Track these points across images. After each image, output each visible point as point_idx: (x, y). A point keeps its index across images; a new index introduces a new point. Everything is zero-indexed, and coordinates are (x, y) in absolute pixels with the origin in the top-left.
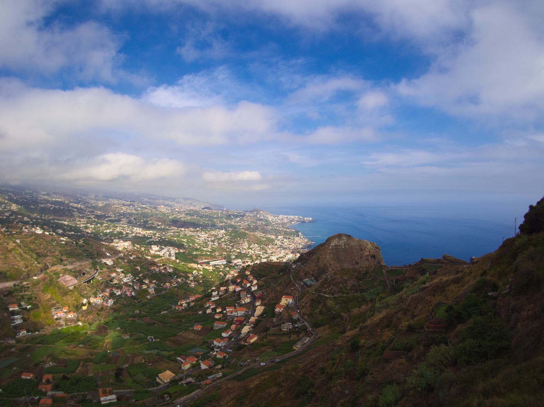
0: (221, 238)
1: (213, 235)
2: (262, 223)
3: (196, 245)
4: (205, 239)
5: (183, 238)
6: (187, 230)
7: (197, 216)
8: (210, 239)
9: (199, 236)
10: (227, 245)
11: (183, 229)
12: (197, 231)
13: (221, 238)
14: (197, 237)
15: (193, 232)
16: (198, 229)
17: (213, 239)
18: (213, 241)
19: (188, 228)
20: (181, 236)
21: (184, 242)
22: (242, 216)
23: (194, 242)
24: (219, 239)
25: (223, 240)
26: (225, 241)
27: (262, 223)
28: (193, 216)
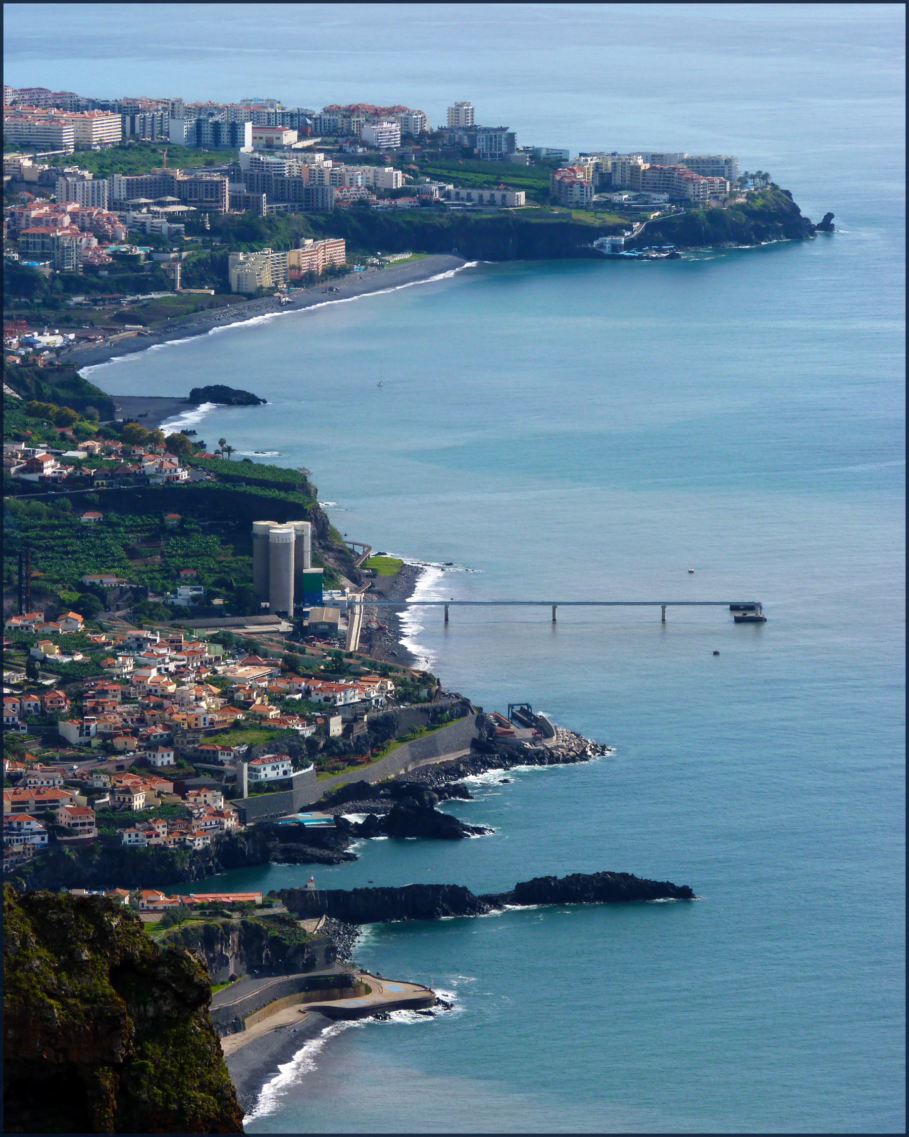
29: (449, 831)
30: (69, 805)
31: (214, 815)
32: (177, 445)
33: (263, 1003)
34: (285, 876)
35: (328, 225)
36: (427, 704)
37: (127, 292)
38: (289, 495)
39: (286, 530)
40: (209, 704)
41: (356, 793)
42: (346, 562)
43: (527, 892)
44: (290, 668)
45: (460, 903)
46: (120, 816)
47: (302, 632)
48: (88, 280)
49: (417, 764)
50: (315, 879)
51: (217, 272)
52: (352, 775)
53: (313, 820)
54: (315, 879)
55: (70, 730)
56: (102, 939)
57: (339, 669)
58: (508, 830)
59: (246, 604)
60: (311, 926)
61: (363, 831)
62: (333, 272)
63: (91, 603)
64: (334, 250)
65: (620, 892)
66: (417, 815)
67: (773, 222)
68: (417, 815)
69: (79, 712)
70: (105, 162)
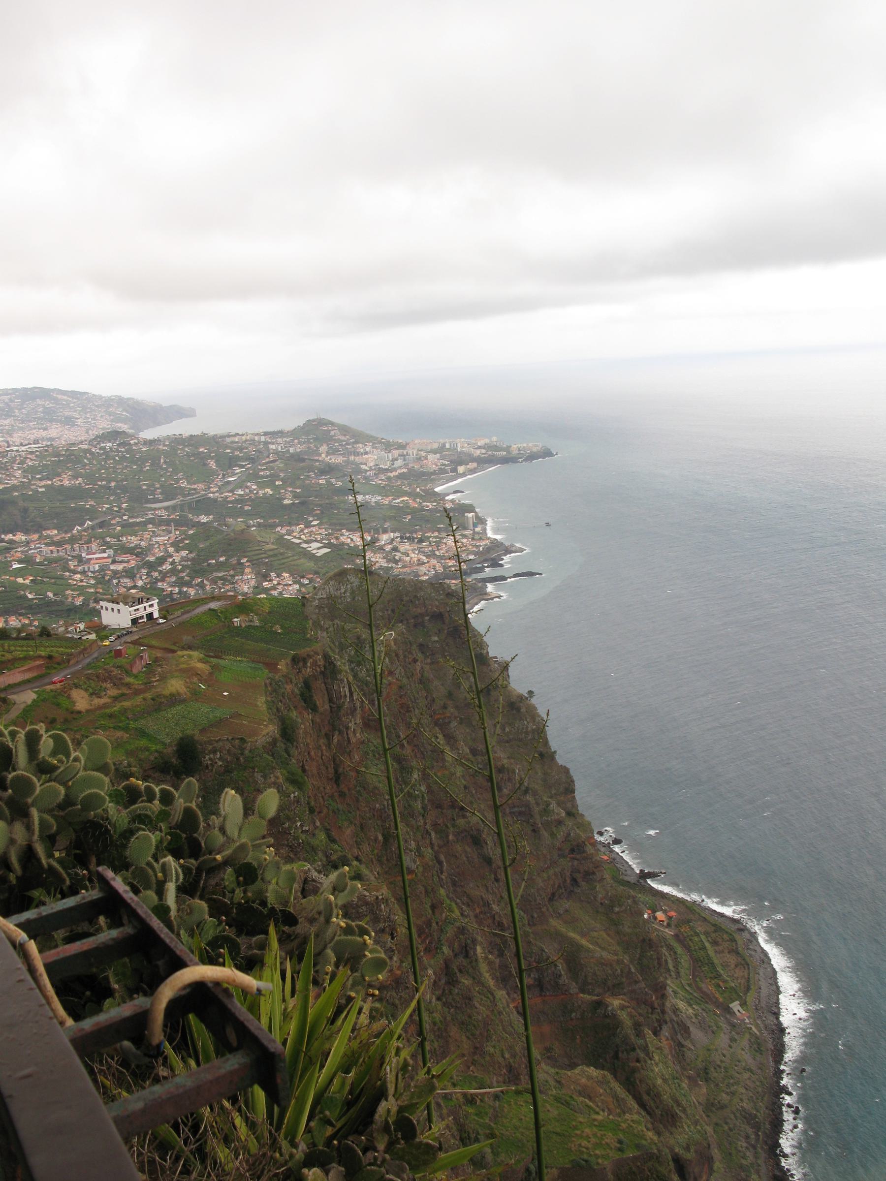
0: (161, 561)
1: (131, 551)
2: (329, 483)
3: (68, 592)
4: (103, 569)
5: (19, 573)
6: (35, 536)
7: (75, 477)
8: (120, 567)
10: (181, 583)
11: (20, 537)
12: (73, 540)
13: (161, 561)
14: (72, 564)
15: (59, 544)
17: (133, 563)
18: (130, 574)
19: (39, 528)
21: (24, 587)
22: (252, 460)
23: (61, 584)
24: (151, 566)
25: (167, 567)
26: (174, 571)
27: (329, 483)
28: (59, 475)
30: (438, 566)
32: (452, 501)
33: (473, 598)
34: (475, 576)
35: (473, 460)
37: (441, 474)
38: (470, 508)
39: (470, 515)
41: (485, 561)
44: (473, 539)
45: (504, 578)
47: (474, 533)
48: (434, 473)
49: (493, 554)
50: (479, 576)
51: (455, 470)
52: (485, 557)
53: (478, 566)
54: (479, 576)
55: (437, 553)
56: (444, 590)
59: (465, 528)
60: (480, 585)
61: (487, 567)
62: (475, 468)
63: (439, 530)
64: (475, 465)
65: (530, 574)
66: (495, 564)
67: (547, 453)
68: (495, 564)
69: (438, 550)
70: (434, 452)
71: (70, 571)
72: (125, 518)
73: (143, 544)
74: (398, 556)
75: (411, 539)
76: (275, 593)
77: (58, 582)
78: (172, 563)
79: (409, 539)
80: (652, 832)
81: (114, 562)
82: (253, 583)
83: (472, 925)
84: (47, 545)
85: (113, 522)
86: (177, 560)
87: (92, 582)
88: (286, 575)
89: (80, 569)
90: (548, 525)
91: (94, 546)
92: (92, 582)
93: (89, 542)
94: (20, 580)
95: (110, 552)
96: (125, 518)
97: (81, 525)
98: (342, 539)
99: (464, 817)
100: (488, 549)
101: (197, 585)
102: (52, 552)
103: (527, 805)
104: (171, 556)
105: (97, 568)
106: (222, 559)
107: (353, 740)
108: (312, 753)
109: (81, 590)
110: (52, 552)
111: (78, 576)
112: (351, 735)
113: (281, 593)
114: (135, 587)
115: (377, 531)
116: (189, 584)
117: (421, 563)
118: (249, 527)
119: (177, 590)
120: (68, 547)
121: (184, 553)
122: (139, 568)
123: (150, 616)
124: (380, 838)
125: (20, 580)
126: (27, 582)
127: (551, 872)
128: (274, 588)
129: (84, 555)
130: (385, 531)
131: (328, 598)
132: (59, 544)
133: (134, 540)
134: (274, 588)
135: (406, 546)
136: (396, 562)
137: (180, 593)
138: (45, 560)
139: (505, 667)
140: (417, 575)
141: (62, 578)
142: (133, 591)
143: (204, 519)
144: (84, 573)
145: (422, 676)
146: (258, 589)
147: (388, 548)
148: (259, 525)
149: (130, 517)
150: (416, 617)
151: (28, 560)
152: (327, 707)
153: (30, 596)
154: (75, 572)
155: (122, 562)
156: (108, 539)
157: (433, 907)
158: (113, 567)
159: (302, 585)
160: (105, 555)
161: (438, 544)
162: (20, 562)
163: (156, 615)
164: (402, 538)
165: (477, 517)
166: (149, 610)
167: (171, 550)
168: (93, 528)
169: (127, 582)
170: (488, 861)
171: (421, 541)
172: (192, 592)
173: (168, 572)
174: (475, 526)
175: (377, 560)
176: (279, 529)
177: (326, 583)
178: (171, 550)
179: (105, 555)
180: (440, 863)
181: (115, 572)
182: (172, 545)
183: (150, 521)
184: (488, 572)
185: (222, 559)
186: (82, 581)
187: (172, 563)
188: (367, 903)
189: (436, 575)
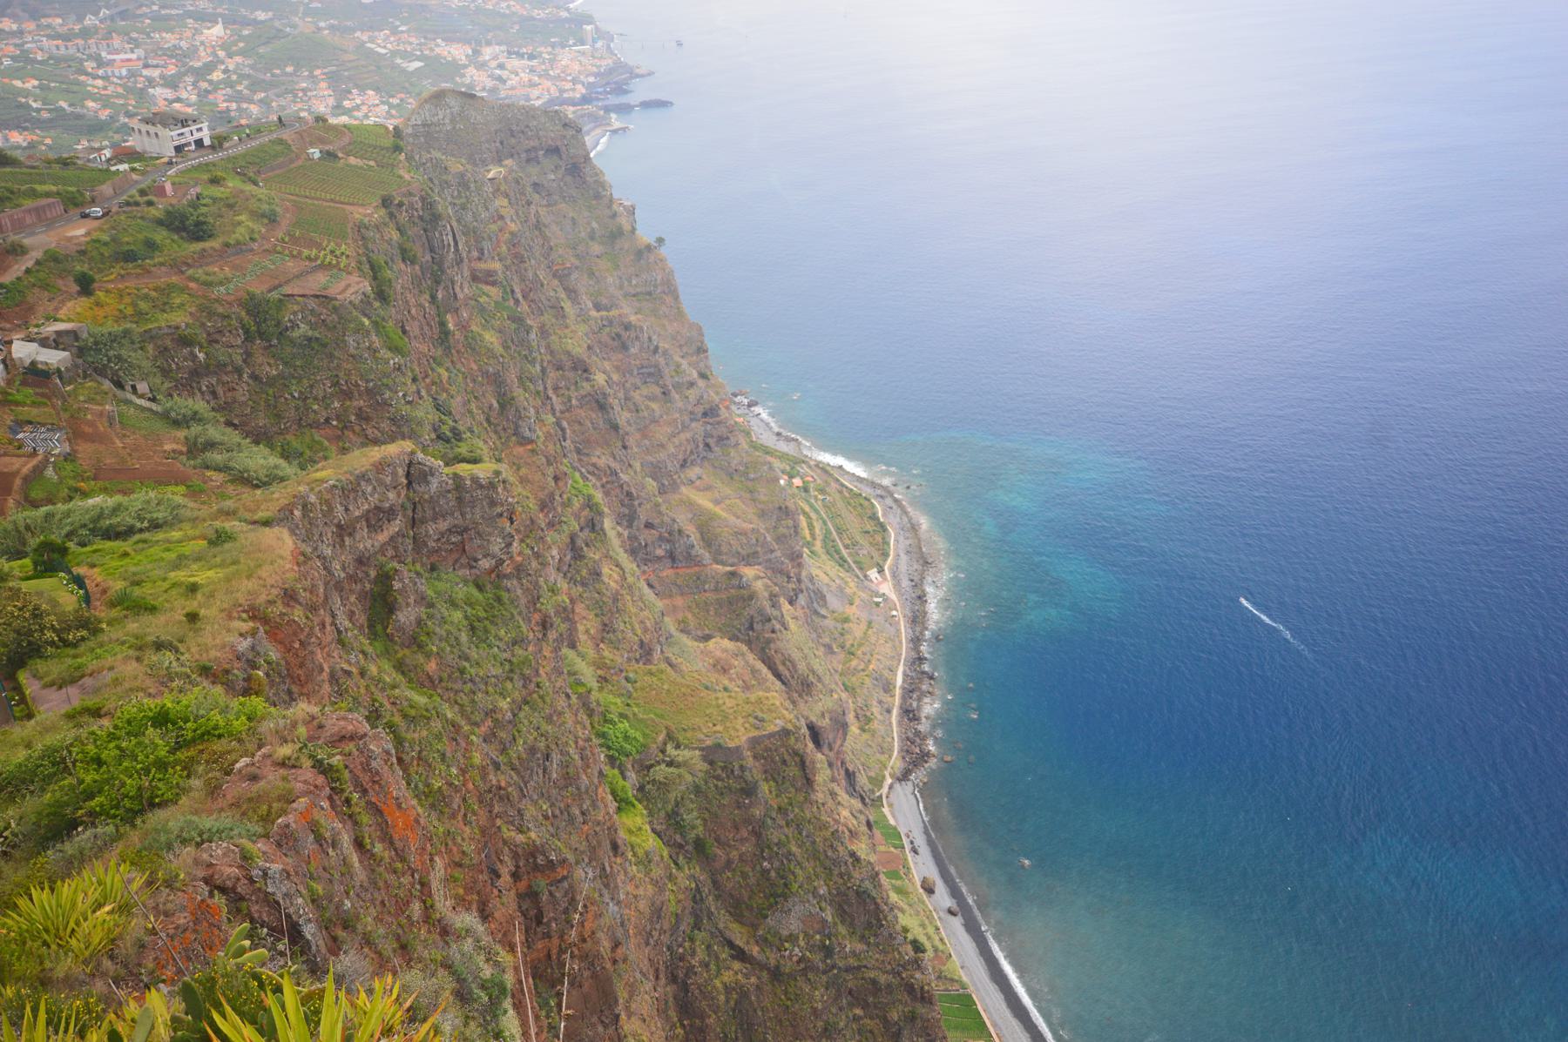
0: (210, 68)
3: (91, 104)
4: (133, 74)
6: (31, 26)
8: (156, 73)
9: (101, 63)
10: (239, 98)
13: (210, 68)
14: (89, 65)
15: (66, 38)
16: (90, 20)
17: (172, 70)
20: (7, 62)
21: (27, 94)
23: (77, 93)
25: (217, 76)
26: (229, 84)
29: (626, 92)
31: (581, 90)
36: (619, 66)
38: (589, 19)
39: (589, 28)
40: (577, 67)
42: (600, 34)
43: (646, 105)
46: (562, 91)
57: (601, 58)
58: (640, 91)
63: (553, 46)
66: (620, 90)
71: (87, 74)
72: (155, 8)
73: (183, 44)
74: (504, 74)
75: (521, 56)
76: (359, 114)
77: (75, 88)
78: (226, 71)
79: (517, 54)
80: (1027, 862)
81: (146, 66)
82: (331, 102)
83: (598, 496)
84: (49, 37)
85: (139, 12)
86: (231, 67)
87: (120, 90)
88: (371, 92)
89: (100, 72)
90: (680, 44)
91: (117, 42)
92: (120, 90)
93: (108, 37)
94: (18, 83)
95: (140, 52)
96: (155, 8)
97: (96, 14)
98: (438, 50)
99: (588, 380)
100: (610, 71)
101: (261, 101)
102: (58, 48)
103: (656, 366)
104: (223, 63)
105: (124, 72)
106: (289, 69)
107: (460, 296)
108: (413, 311)
109: (105, 101)
110: (58, 48)
111: (99, 83)
112: (457, 289)
113: (366, 116)
114: (178, 100)
115: (479, 43)
116: (251, 101)
117: (532, 85)
118: (319, 29)
119: (234, 106)
120: (81, 42)
121: (238, 59)
122: (180, 75)
123: (199, 143)
124: (496, 405)
125: (18, 83)
126: (28, 85)
127: (683, 436)
128: (357, 108)
129: (104, 54)
130: (489, 43)
131: (424, 125)
132: (66, 38)
133: (169, 39)
134: (357, 108)
135: (515, 63)
136: (504, 82)
137: (239, 109)
138: (50, 58)
139: (631, 211)
140: (528, 99)
141: (78, 83)
142: (177, 106)
143: (261, 16)
144: (106, 78)
145: (552, 352)
146: (338, 109)
147: (494, 64)
148: (331, 27)
149: (162, 7)
150: (528, 151)
151: (25, 58)
152: (428, 257)
153: (34, 105)
154: (96, 77)
155: (157, 66)
156: (134, 35)
157: (556, 479)
158: (145, 72)
159: (391, 106)
160: (134, 56)
161: (553, 61)
162: (13, 58)
163: (207, 142)
164: (509, 53)
165: (597, 29)
166: (197, 136)
167: (221, 54)
168: (112, 18)
169: (168, 93)
170: (615, 428)
171: (531, 57)
172: (254, 109)
173: (219, 82)
174: (594, 41)
175: (478, 80)
176: (358, 34)
177: (421, 106)
178: (221, 54)
179: (134, 56)
180: (563, 430)
181: (151, 82)
182: (223, 47)
183: (189, 15)
184: (614, 100)
185: (289, 69)
186: (105, 88)
187: (226, 71)
188: (481, 487)
189: (551, 101)
